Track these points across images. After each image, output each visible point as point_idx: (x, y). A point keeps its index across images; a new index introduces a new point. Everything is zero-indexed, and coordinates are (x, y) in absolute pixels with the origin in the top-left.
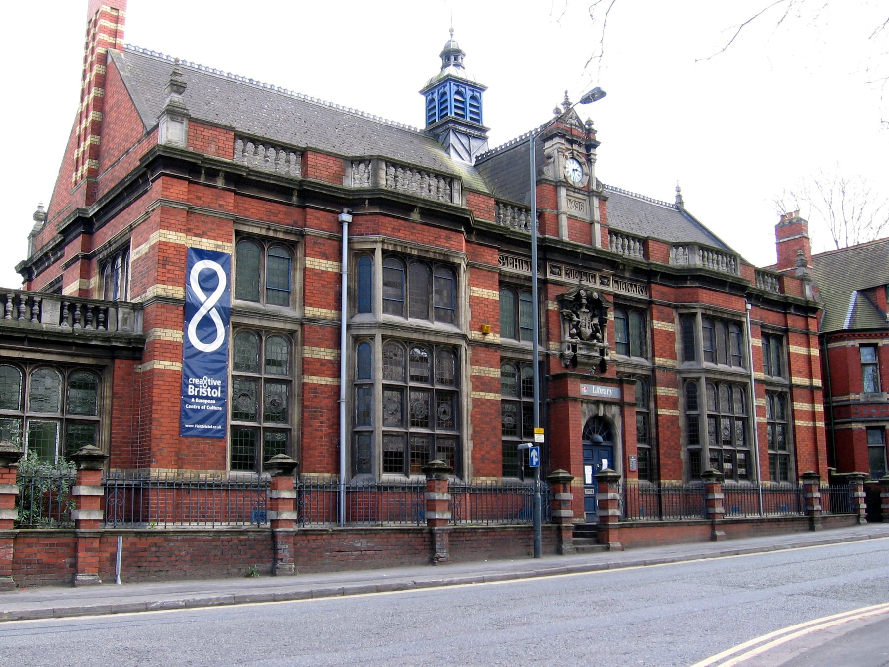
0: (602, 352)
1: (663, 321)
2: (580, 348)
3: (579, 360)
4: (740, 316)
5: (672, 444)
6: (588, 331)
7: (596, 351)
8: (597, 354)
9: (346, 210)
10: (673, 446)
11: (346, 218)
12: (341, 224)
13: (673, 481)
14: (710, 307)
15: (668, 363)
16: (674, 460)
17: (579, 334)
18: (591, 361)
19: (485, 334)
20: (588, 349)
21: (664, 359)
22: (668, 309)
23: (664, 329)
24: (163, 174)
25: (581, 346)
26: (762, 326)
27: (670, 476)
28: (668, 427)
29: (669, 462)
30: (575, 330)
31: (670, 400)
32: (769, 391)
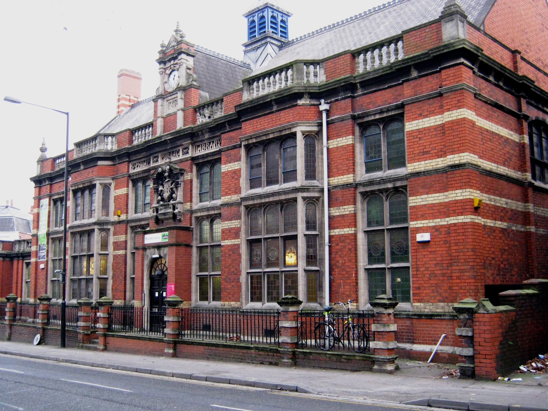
0: (174, 208)
1: (230, 163)
2: (161, 210)
3: (159, 218)
4: (290, 128)
5: (233, 270)
6: (166, 195)
7: (170, 208)
8: (171, 210)
9: (323, 101)
10: (233, 272)
11: (324, 106)
12: (321, 113)
13: (232, 303)
14: (251, 136)
15: (232, 199)
16: (234, 284)
17: (163, 200)
18: (167, 217)
19: (119, 216)
20: (165, 208)
21: (229, 197)
22: (235, 150)
23: (231, 169)
24: (462, 64)
25: (161, 208)
26: (354, 118)
27: (230, 298)
28: (230, 255)
29: (229, 286)
30: (159, 198)
31: (232, 231)
32: (367, 192)
